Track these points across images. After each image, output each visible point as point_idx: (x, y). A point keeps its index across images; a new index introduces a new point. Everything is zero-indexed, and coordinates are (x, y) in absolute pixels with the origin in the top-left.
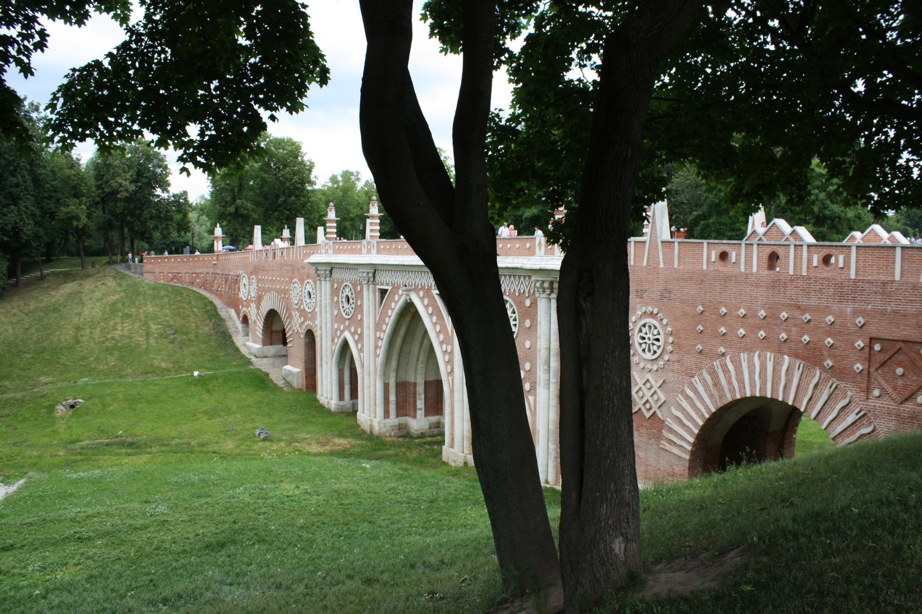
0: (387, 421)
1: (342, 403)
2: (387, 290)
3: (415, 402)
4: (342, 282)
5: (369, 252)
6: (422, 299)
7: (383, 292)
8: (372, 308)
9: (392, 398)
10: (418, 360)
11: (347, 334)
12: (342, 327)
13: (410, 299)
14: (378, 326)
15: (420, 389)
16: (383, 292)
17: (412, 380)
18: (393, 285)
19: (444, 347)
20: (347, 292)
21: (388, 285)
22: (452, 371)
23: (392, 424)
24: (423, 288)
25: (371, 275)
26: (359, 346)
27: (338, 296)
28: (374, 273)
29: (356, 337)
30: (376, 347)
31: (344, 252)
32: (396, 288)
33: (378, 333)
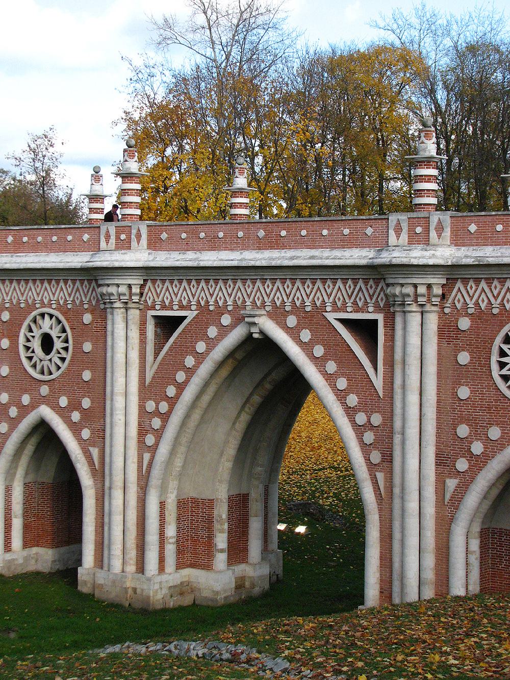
0: (164, 577)
1: (8, 556)
2: (185, 318)
3: (211, 537)
4: (32, 307)
5: (124, 245)
6: (294, 333)
7: (167, 325)
8: (134, 355)
9: (171, 531)
10: (221, 454)
11: (45, 411)
12: (26, 399)
13: (261, 332)
14: (146, 391)
15: (222, 511)
16: (167, 325)
17: (207, 495)
18: (203, 309)
19: (361, 418)
20: (46, 325)
21: (188, 307)
22: (388, 458)
23: (171, 584)
24: (297, 310)
25: (136, 290)
26: (86, 434)
27: (14, 338)
28: (142, 287)
29: (76, 416)
30: (142, 432)
31: (35, 248)
32: (208, 315)
33: (150, 406)
